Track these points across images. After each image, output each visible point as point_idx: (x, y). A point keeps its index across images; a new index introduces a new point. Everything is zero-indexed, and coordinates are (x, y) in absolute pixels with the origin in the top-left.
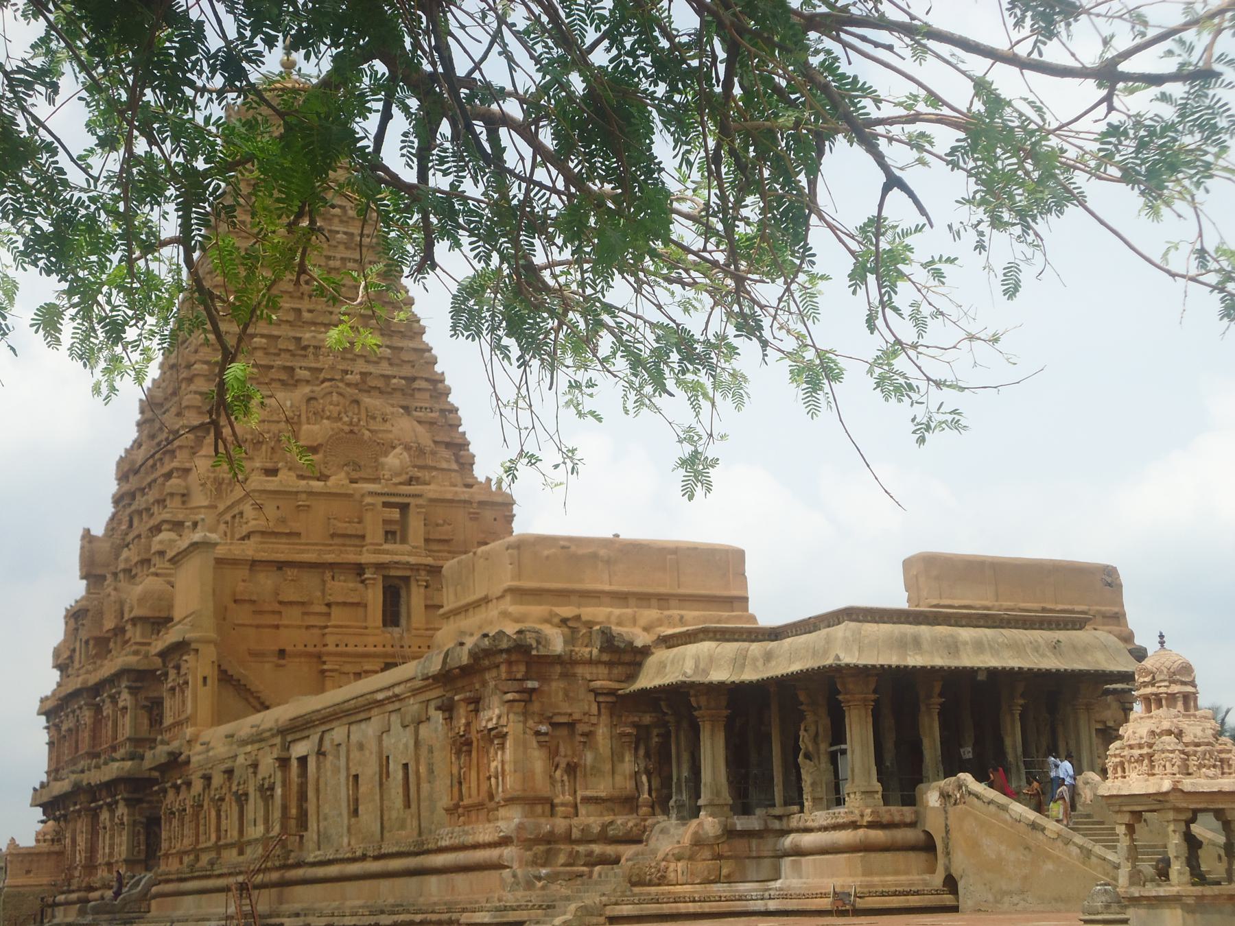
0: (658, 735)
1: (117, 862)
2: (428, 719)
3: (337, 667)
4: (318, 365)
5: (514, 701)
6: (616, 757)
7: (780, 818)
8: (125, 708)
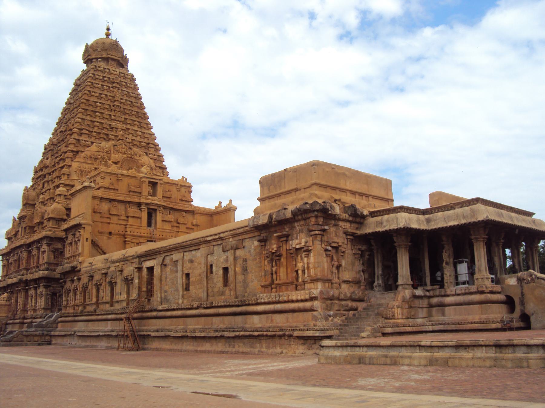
0: (368, 255)
1: (39, 309)
2: (244, 247)
6: (353, 264)
7: (428, 291)
8: (45, 251)
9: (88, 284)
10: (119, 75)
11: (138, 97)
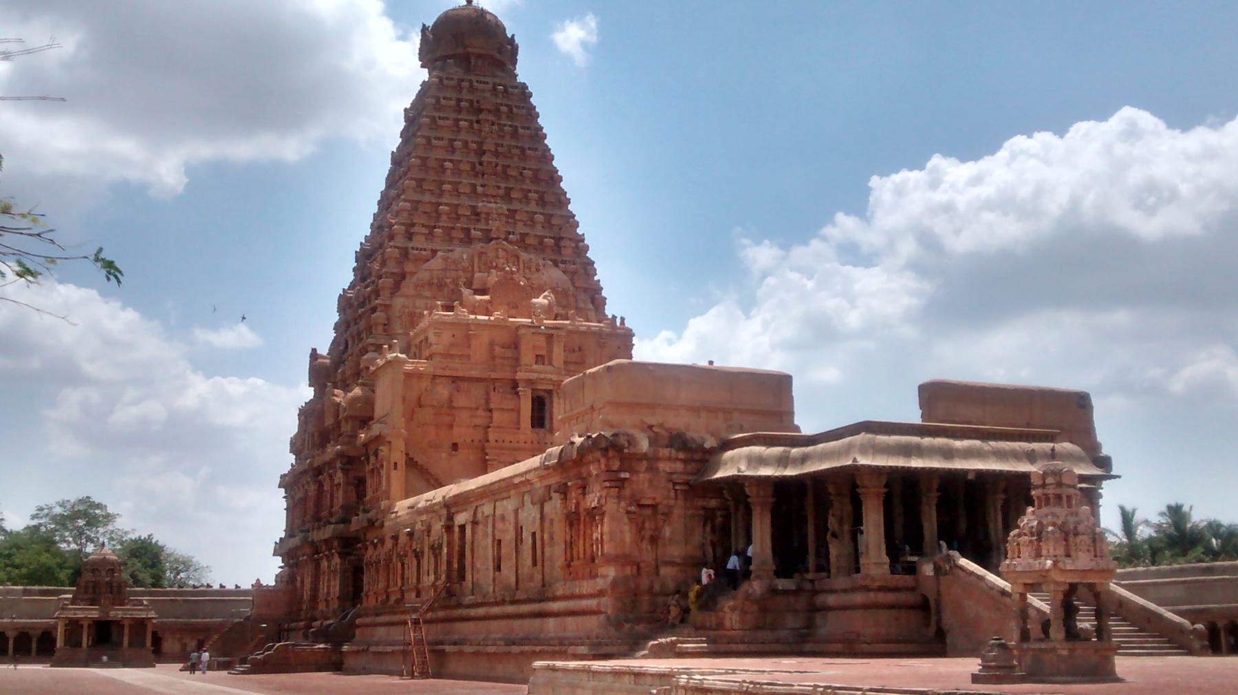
0: (721, 516)
1: (332, 599)
2: (550, 499)
3: (496, 457)
4: (489, 228)
5: (610, 487)
8: (339, 484)
9: (391, 553)
10: (494, 89)
11: (537, 135)
